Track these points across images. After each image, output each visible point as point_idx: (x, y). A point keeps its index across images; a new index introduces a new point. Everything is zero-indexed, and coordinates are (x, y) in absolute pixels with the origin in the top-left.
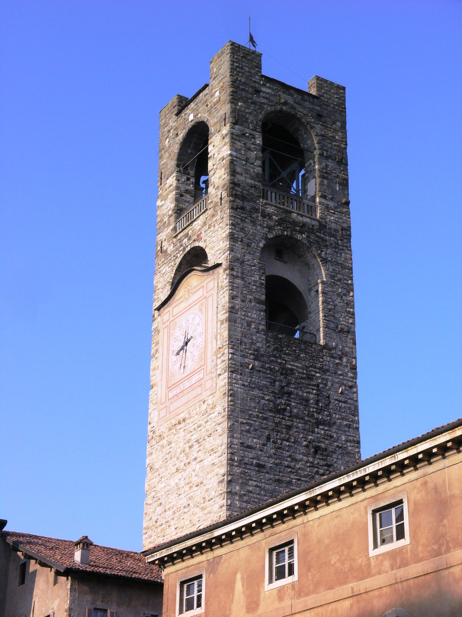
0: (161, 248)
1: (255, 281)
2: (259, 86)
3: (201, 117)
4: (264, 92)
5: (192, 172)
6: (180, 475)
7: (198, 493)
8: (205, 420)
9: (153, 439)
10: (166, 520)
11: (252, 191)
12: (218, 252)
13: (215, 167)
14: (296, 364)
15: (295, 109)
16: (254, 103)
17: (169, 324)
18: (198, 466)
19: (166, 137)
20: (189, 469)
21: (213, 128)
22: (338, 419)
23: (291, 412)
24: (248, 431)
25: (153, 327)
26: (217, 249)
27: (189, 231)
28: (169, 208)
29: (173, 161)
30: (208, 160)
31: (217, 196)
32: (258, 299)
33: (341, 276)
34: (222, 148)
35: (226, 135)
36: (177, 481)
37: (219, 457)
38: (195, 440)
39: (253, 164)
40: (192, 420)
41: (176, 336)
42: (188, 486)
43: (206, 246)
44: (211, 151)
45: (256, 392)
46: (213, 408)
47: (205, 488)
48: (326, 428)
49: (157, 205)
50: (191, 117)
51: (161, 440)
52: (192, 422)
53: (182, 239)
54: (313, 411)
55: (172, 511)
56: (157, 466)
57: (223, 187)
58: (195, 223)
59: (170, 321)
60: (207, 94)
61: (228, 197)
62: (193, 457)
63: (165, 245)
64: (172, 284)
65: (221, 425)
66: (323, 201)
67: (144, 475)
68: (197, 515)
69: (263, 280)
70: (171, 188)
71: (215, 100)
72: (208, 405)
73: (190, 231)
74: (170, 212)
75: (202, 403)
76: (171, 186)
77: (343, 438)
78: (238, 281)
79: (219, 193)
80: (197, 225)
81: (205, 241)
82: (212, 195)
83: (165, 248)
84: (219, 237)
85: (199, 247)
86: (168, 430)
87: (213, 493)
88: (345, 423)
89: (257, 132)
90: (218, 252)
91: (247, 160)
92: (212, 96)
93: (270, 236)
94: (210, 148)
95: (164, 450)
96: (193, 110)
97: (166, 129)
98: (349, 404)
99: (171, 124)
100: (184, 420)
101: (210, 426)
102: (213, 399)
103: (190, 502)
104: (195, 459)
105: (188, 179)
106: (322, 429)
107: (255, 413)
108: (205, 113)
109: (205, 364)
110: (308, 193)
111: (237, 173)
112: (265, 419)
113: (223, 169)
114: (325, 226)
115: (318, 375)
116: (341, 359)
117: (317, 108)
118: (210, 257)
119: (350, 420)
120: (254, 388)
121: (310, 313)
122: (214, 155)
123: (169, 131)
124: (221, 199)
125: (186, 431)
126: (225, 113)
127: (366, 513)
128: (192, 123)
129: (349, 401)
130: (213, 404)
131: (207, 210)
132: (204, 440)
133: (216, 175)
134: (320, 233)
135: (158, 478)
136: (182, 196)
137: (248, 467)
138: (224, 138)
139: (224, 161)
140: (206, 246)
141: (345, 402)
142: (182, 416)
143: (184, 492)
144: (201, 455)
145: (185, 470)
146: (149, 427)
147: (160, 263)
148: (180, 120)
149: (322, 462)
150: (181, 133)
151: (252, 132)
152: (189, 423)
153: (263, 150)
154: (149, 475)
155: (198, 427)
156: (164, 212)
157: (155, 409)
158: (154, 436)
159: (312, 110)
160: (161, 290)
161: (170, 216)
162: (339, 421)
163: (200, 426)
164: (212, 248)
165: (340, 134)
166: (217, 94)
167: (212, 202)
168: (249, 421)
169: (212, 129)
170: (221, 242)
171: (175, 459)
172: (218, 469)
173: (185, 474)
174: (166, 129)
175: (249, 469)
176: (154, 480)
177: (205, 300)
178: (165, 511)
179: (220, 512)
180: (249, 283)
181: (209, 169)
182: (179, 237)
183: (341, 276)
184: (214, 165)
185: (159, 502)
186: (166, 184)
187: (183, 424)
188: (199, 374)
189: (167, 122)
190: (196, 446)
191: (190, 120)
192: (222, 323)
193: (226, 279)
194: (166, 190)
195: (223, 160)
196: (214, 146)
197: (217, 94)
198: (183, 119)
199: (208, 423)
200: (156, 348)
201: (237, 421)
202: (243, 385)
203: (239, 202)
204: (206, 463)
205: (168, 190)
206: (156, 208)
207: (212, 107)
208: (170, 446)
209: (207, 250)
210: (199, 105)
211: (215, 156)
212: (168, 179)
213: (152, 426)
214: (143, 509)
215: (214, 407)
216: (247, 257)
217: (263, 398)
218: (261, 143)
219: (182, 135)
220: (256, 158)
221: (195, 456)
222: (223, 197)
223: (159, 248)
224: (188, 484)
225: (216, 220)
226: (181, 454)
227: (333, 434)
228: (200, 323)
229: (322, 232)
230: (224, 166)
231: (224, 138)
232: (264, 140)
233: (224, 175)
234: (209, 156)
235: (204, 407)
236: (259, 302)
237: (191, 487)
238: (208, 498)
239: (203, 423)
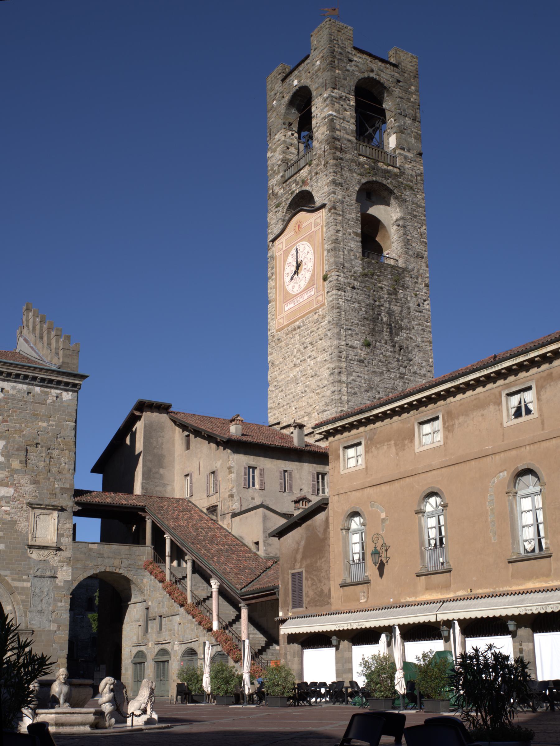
0: (273, 191)
1: (353, 218)
2: (352, 57)
3: (304, 82)
4: (356, 61)
5: (296, 129)
6: (297, 369)
7: (313, 383)
8: (317, 327)
9: (273, 342)
10: (287, 402)
11: (349, 144)
12: (323, 195)
13: (318, 125)
14: (385, 283)
15: (379, 76)
16: (348, 70)
17: (281, 252)
18: (312, 362)
19: (273, 99)
20: (304, 365)
21: (315, 92)
22: (416, 325)
23: (382, 320)
24: (351, 335)
25: (269, 255)
26: (322, 192)
27: (298, 177)
28: (278, 159)
29: (280, 120)
30: (311, 119)
31: (320, 149)
32: (356, 232)
33: (417, 214)
34: (323, 109)
35: (327, 98)
36: (295, 373)
37: (330, 355)
38: (309, 343)
39: (348, 122)
40: (306, 327)
42: (304, 377)
43: (313, 190)
44: (314, 111)
45: (356, 305)
46: (323, 318)
47: (319, 378)
48: (407, 332)
49: (268, 156)
50: (296, 82)
51: (280, 342)
52: (306, 329)
53: (291, 184)
54: (398, 319)
55: (292, 396)
56: (278, 363)
57: (326, 141)
58: (302, 171)
60: (309, 63)
61: (330, 149)
62: (308, 356)
63: (277, 189)
64: (283, 220)
65: (331, 331)
66: (402, 152)
67: (267, 369)
68: (313, 399)
69: (359, 217)
70: (279, 142)
71: (316, 68)
72: (319, 315)
73: (298, 178)
74: (279, 162)
75: (313, 313)
76: (279, 140)
77: (419, 339)
78: (340, 218)
79: (323, 147)
80: (304, 173)
81: (312, 186)
82: (317, 148)
83: (276, 191)
84: (324, 183)
85: (306, 190)
86: (285, 335)
87: (326, 382)
88: (421, 328)
89: (351, 95)
90: (323, 195)
91: (344, 119)
92: (313, 65)
93: (364, 180)
94: (313, 109)
95: (283, 350)
96: (297, 77)
97: (273, 93)
98: (424, 313)
99: (277, 89)
100: (299, 327)
101: (321, 332)
103: (306, 389)
104: (310, 357)
105: (293, 135)
106: (405, 333)
107: (355, 322)
108: (307, 79)
110: (390, 146)
111: (337, 130)
112: (364, 326)
113: (326, 127)
114: (404, 173)
115: (401, 291)
116: (417, 278)
117: (397, 75)
118: (316, 199)
119: (425, 326)
120: (355, 302)
121: (393, 243)
122: (317, 115)
123: (276, 94)
124: (324, 151)
125: (301, 336)
126: (326, 80)
127: (501, 396)
128: (297, 88)
129: (424, 311)
130: (323, 315)
131: (312, 160)
132: (316, 342)
133: (319, 132)
134: (401, 178)
135: (279, 372)
136: (288, 148)
137: (352, 362)
138: (325, 101)
139: (326, 120)
140: (313, 190)
141: (421, 312)
142: (297, 323)
143: (301, 382)
144: (314, 354)
145: (301, 365)
146: (269, 333)
147: (272, 204)
148: (286, 85)
149: (405, 358)
150: (287, 96)
151: (348, 95)
152: (302, 330)
153: (356, 111)
154: (271, 369)
155: (311, 332)
156: (275, 161)
158: (273, 340)
159: (392, 76)
160: (274, 225)
161: (280, 165)
162: (417, 326)
163: (313, 332)
164: (318, 192)
165: (414, 96)
166: (318, 63)
167: (316, 154)
168: (351, 327)
169: (314, 93)
170: (326, 187)
171: (293, 357)
172: (330, 364)
173: (301, 368)
174: (273, 93)
175: (353, 364)
176: (276, 373)
177: (313, 233)
178: (286, 396)
179: (332, 396)
180: (349, 220)
181: (313, 126)
182: (288, 183)
183: (417, 214)
184: (317, 123)
185: (280, 389)
186: (275, 139)
187: (298, 330)
188: (311, 292)
189: (273, 86)
190: (310, 347)
191: (294, 85)
192: (329, 251)
193: (331, 216)
194: (275, 144)
195: (325, 119)
196: (316, 107)
197: (318, 63)
198: (287, 84)
199: (319, 330)
200: (272, 271)
201: (343, 328)
202: (347, 300)
203: (338, 154)
204: (318, 359)
205: (276, 144)
206: (266, 159)
207: (313, 74)
208: (288, 347)
209: (314, 194)
210: (303, 73)
211: (318, 116)
212: (276, 134)
213: (271, 332)
214: (267, 395)
215: (324, 317)
216: (347, 199)
217: (361, 310)
218: (354, 104)
219: (287, 97)
220: (352, 117)
221: (309, 355)
222: (326, 149)
223: (271, 192)
224: (304, 375)
225: (321, 169)
226: (297, 353)
227: (412, 336)
228: (310, 252)
229: (402, 177)
230: (326, 124)
231: (325, 101)
232: (357, 102)
233: (326, 131)
234: (312, 115)
235: (316, 317)
236: (356, 234)
237: (307, 378)
238: (321, 386)
239: (315, 329)
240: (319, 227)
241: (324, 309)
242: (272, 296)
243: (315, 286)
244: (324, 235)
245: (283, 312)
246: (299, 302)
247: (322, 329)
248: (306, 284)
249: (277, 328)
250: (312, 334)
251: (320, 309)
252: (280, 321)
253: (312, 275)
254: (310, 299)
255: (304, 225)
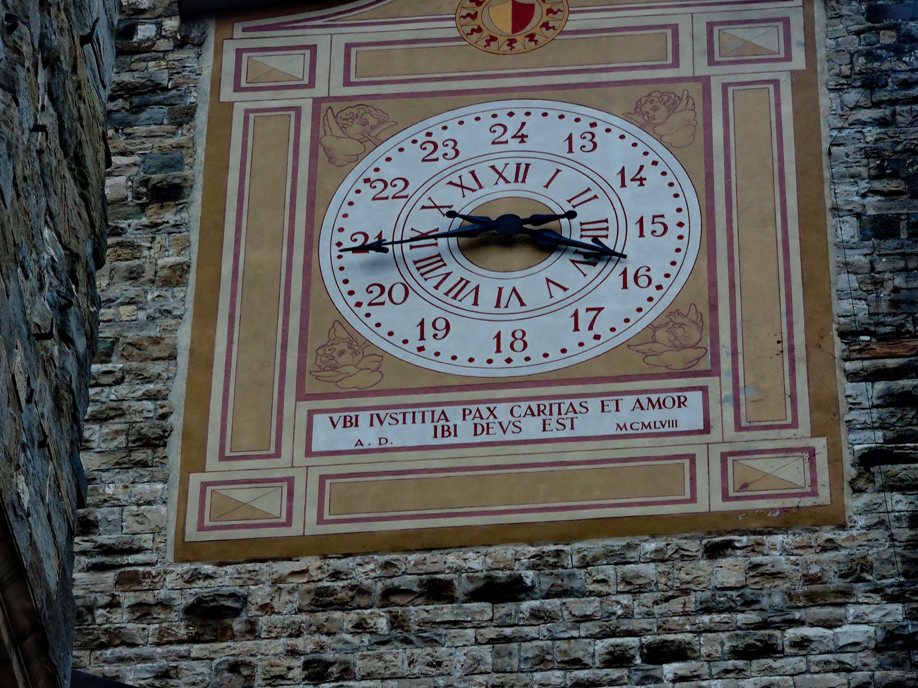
17: (304, 100)
40: (579, 606)
41: (389, 172)
46: (813, 599)
59: (320, 90)
75: (693, 546)
102: (809, 556)
109: (714, 371)
130: (810, 580)
157: (144, 464)
158: (128, 599)
188: (661, 404)
240: (781, 72)
241: (831, 546)
242: (133, 323)
243: (721, 386)
244: (826, 135)
245: (293, 447)
246: (497, 435)
247: (798, 663)
248: (595, 350)
249: (192, 534)
250: (669, 669)
251: (779, 538)
252: (242, 495)
253: (672, 312)
254: (641, 447)
255: (576, 21)
